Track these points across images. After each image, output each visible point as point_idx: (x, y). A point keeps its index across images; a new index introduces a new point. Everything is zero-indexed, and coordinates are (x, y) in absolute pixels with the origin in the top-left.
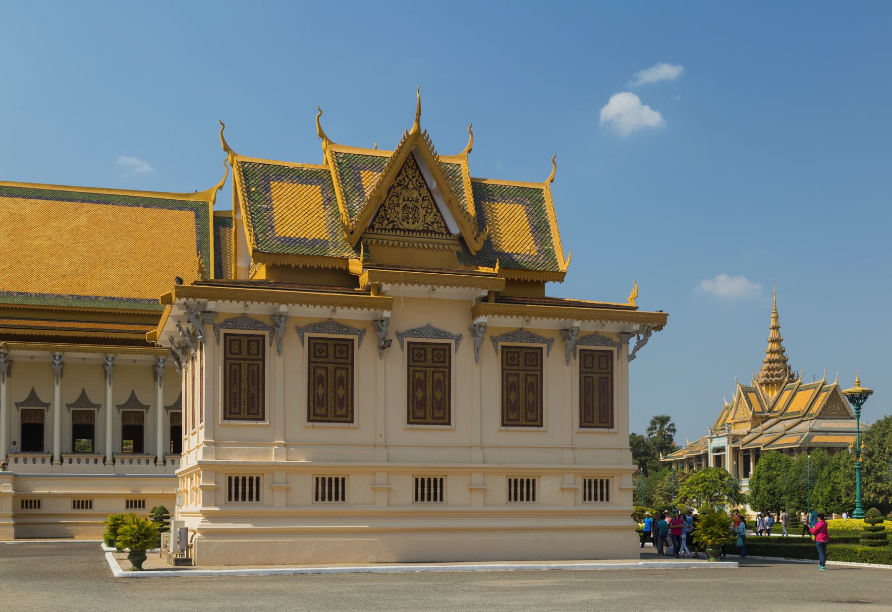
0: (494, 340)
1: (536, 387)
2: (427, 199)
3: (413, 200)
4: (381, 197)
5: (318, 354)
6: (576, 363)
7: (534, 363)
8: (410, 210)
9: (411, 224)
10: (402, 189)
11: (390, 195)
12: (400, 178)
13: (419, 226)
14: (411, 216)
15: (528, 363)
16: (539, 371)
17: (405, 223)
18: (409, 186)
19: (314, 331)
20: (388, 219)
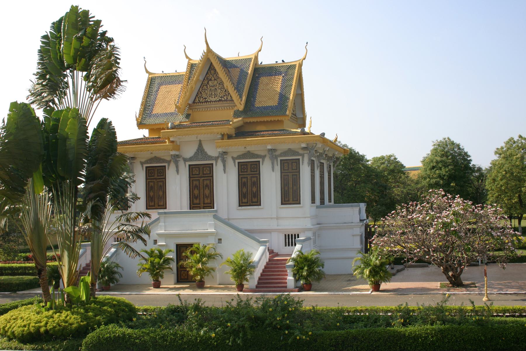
0: (234, 159)
1: (257, 184)
2: (221, 83)
3: (214, 86)
4: (192, 88)
5: (150, 175)
6: (278, 168)
7: (255, 170)
8: (213, 91)
9: (213, 98)
10: (208, 81)
11: (203, 85)
12: (208, 75)
13: (217, 99)
14: (213, 94)
15: (252, 170)
16: (258, 174)
17: (211, 98)
18: (212, 79)
19: (148, 163)
20: (202, 97)
